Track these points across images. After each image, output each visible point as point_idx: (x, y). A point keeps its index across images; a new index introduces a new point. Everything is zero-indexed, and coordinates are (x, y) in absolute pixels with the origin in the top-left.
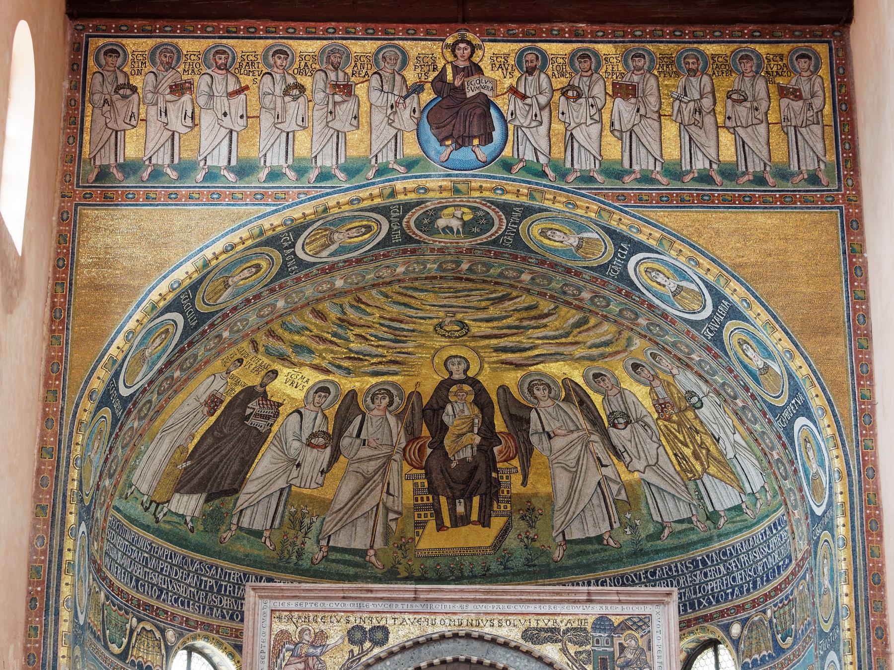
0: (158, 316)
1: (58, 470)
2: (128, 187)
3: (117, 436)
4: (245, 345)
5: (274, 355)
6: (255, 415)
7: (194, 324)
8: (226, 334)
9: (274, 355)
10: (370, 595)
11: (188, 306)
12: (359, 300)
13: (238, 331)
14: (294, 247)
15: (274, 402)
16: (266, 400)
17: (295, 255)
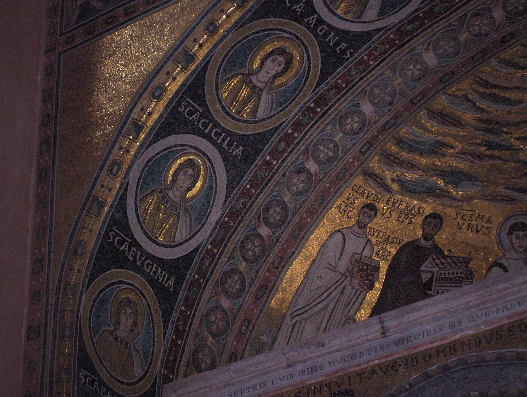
0: (155, 140)
1: (45, 348)
2: (107, 13)
3: (184, 317)
4: (359, 180)
5: (420, 192)
6: (439, 280)
7: (239, 151)
8: (312, 166)
9: (420, 192)
10: (322, 350)
11: (205, 125)
12: (486, 84)
13: (330, 160)
14: (314, 11)
15: (457, 258)
16: (444, 257)
17: (328, 25)
